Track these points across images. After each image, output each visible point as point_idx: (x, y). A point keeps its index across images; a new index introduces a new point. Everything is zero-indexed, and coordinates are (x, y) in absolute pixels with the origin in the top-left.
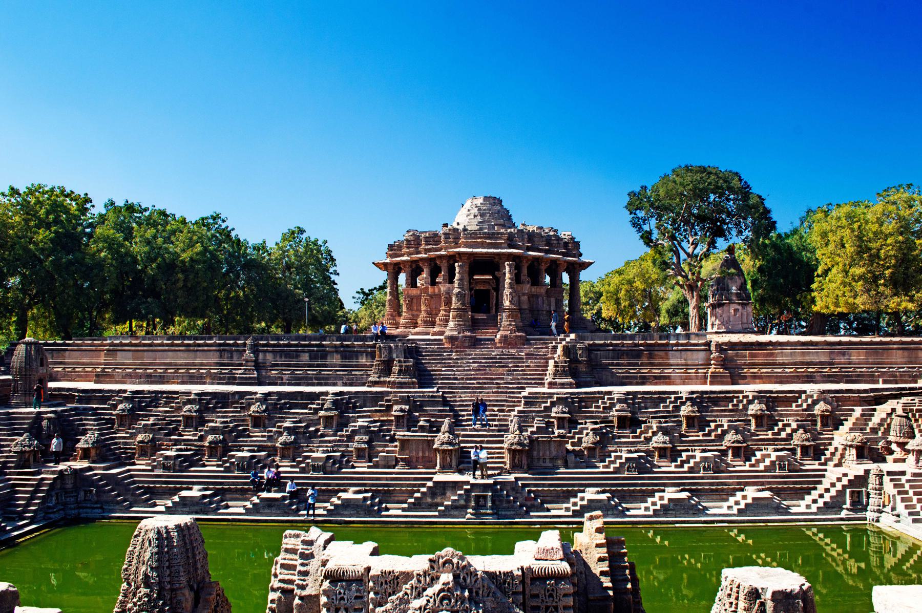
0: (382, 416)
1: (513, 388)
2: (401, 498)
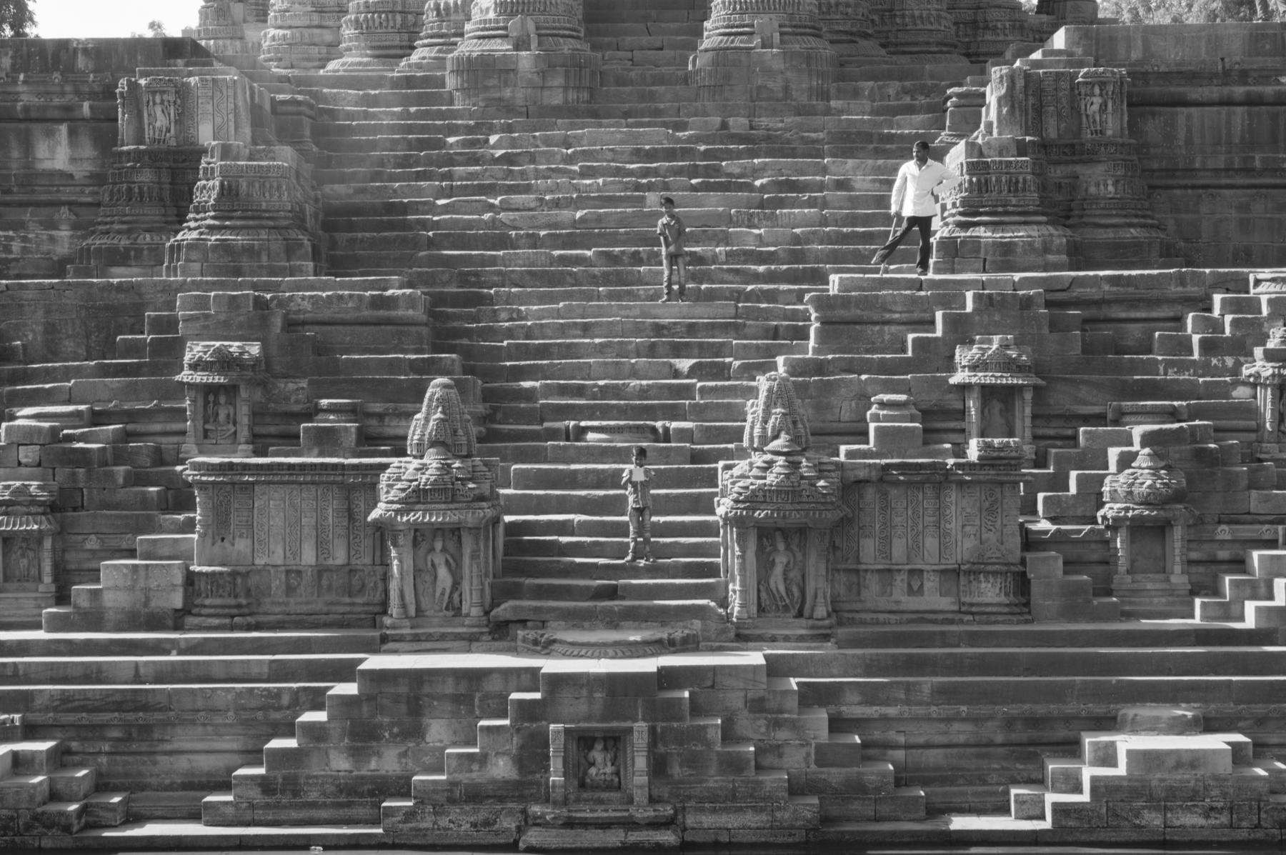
0: (131, 392)
1: (771, 277)
2: (205, 763)
